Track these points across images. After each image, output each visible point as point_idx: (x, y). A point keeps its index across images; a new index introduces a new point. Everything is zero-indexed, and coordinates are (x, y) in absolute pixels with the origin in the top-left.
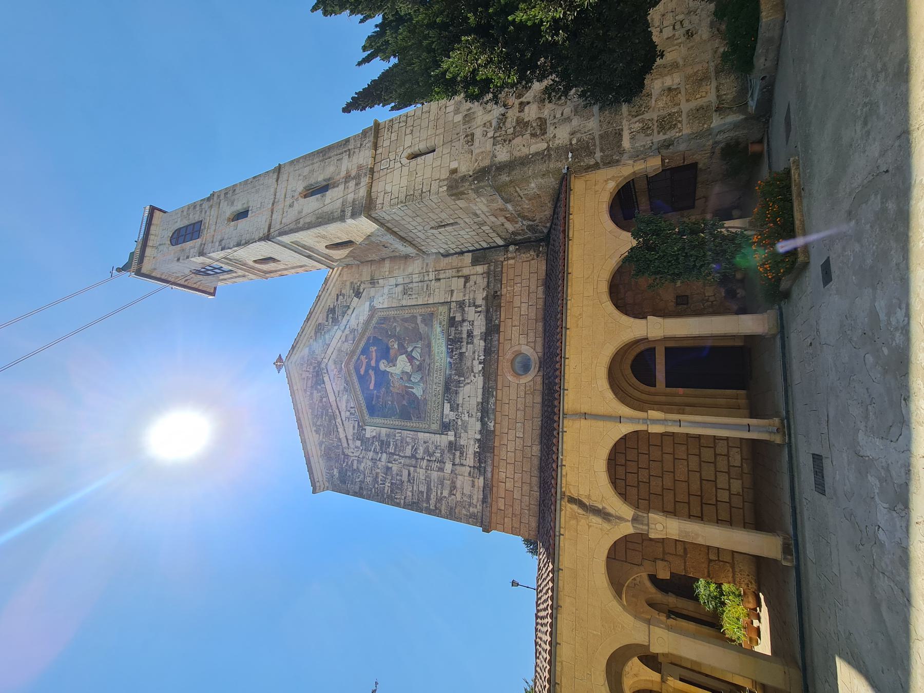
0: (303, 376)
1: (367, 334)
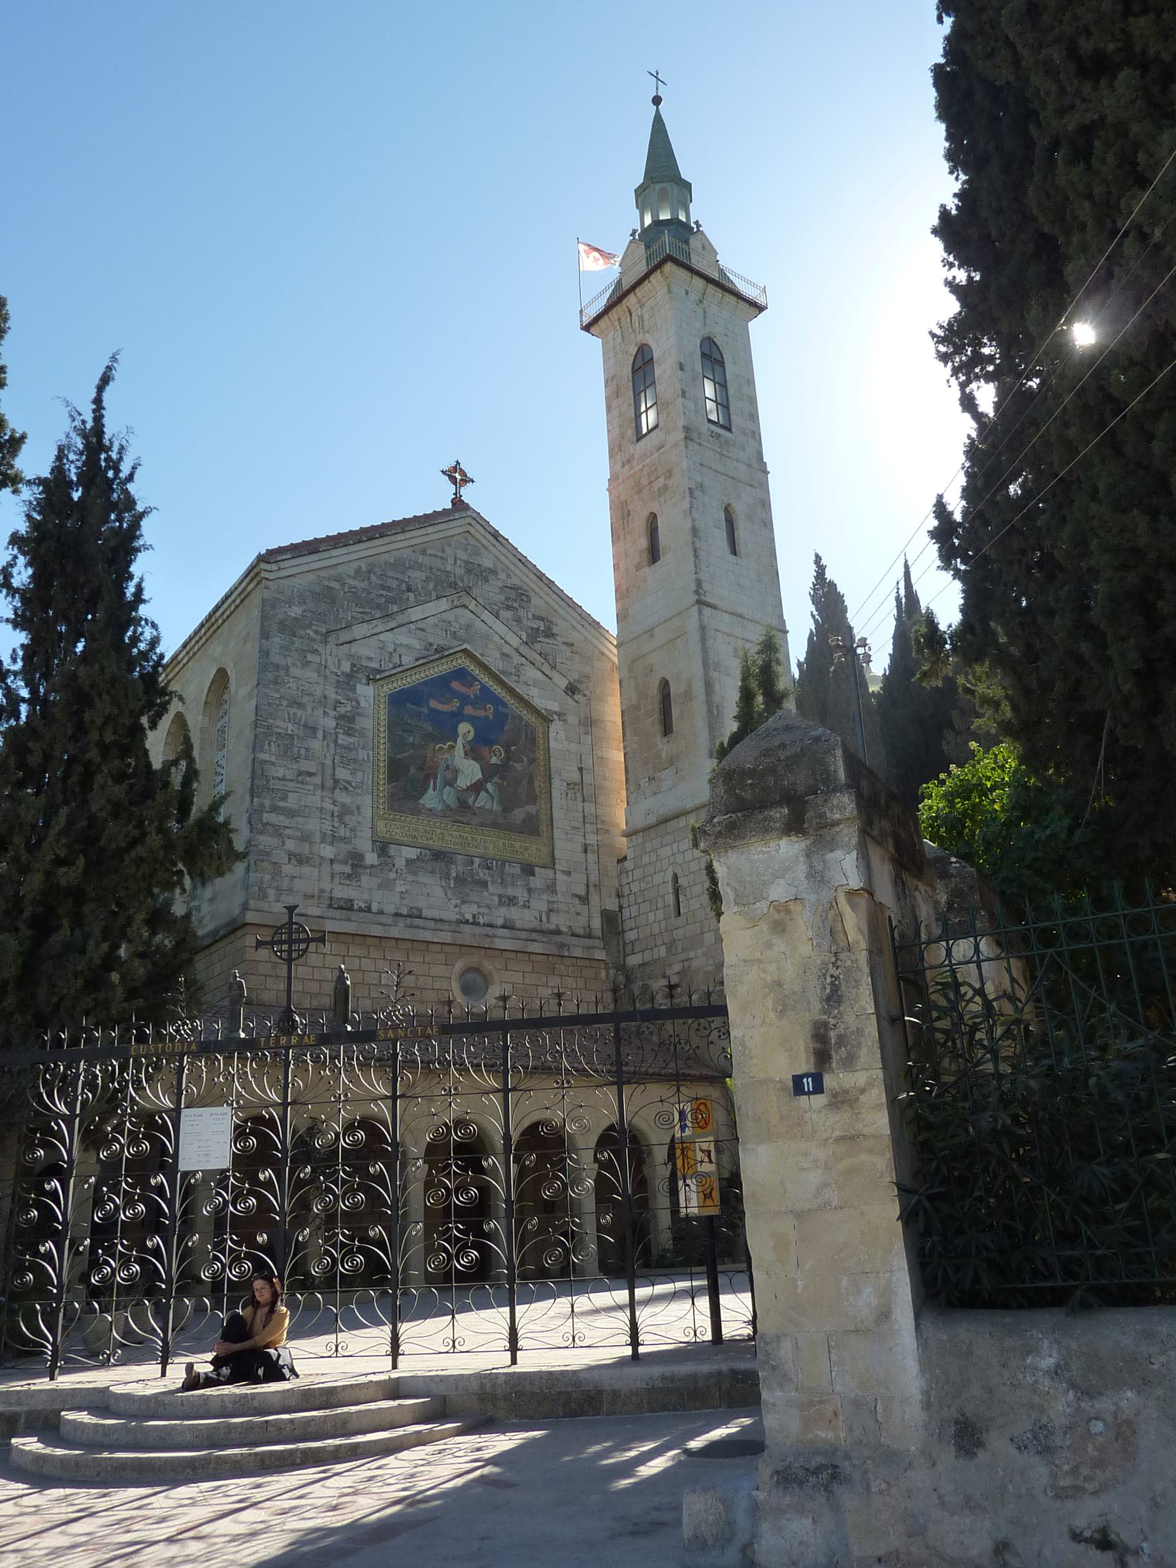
0: (448, 549)
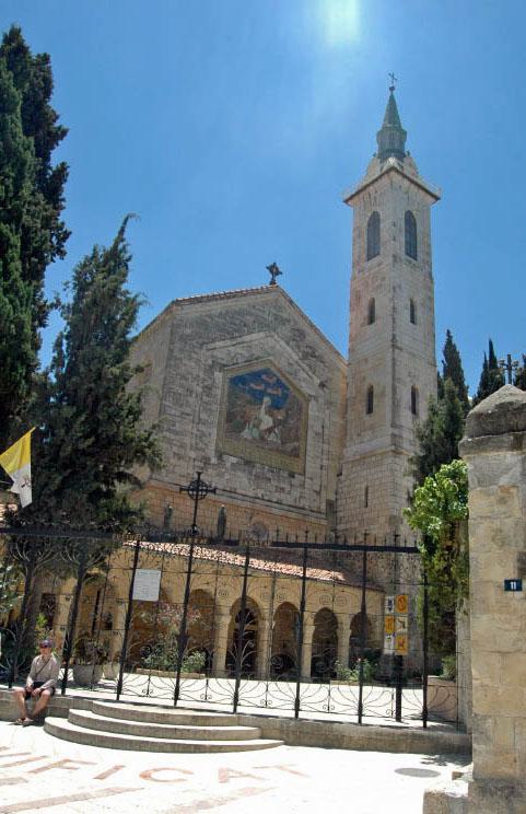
1: (292, 389)
